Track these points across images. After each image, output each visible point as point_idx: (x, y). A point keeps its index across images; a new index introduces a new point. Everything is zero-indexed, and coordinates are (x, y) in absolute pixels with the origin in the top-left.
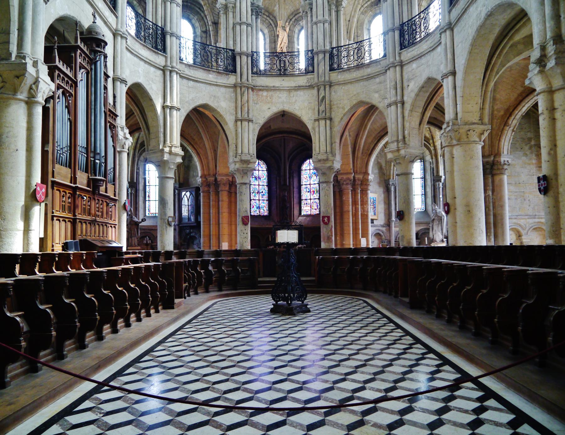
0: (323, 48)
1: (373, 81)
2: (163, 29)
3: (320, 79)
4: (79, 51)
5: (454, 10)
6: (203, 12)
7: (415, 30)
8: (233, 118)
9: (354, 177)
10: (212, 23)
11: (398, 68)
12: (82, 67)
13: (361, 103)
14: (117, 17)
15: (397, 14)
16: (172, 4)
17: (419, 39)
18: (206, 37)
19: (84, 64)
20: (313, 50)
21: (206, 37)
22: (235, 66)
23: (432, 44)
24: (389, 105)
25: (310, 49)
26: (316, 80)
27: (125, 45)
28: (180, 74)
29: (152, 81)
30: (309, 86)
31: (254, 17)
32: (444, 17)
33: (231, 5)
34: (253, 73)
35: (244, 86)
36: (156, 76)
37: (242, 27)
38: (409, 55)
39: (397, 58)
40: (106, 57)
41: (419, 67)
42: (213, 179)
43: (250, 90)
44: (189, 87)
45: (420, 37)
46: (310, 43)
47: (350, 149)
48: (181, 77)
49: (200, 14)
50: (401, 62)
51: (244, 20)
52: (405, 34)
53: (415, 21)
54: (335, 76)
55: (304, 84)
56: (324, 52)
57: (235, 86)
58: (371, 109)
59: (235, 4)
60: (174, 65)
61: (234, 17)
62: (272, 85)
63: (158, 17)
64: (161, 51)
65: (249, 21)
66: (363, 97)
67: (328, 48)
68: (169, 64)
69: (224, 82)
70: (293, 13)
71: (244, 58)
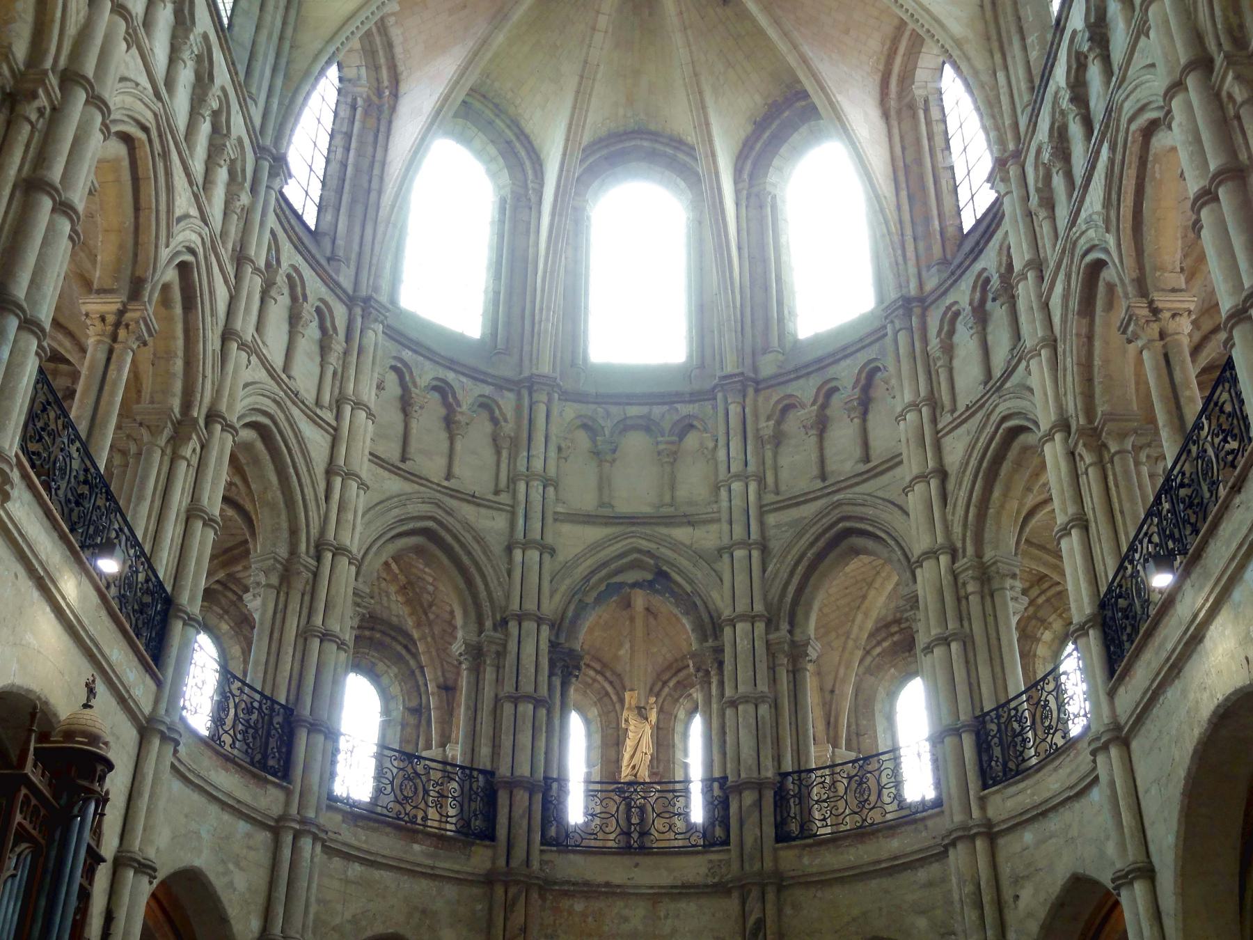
0: (755, 775)
1: (908, 876)
2: (289, 711)
3: (747, 866)
4: (24, 791)
5: (1121, 690)
6: (415, 656)
7: (1020, 734)
10: (439, 687)
11: (979, 843)
12: (22, 835)
14: (159, 684)
16: (326, 644)
17: (1034, 761)
18: (418, 726)
19: (29, 827)
20: (725, 778)
21: (418, 726)
23: (1074, 779)
25: (717, 775)
26: (735, 866)
27: (169, 758)
28: (323, 841)
29: (237, 865)
30: (715, 885)
31: (557, 682)
32: (1096, 706)
33: (494, 648)
34: (545, 841)
35: (517, 882)
36: (250, 848)
37: (521, 708)
38: (1010, 804)
39: (976, 813)
40: (103, 800)
41: (1044, 841)
43: (535, 895)
44: (347, 881)
45: (1037, 754)
46: (716, 757)
48: (327, 849)
49: (407, 663)
50: (989, 824)
51: (527, 687)
52: (995, 744)
53: (1016, 709)
54: (792, 859)
55: (700, 880)
56: (759, 786)
57: (489, 880)
59: (505, 646)
60: (311, 814)
61: (498, 681)
62: (600, 879)
63: (279, 678)
64: (274, 775)
65: (544, 691)
67: (769, 773)
68: (294, 811)
69: (457, 867)
70: (669, 667)
71: (521, 797)
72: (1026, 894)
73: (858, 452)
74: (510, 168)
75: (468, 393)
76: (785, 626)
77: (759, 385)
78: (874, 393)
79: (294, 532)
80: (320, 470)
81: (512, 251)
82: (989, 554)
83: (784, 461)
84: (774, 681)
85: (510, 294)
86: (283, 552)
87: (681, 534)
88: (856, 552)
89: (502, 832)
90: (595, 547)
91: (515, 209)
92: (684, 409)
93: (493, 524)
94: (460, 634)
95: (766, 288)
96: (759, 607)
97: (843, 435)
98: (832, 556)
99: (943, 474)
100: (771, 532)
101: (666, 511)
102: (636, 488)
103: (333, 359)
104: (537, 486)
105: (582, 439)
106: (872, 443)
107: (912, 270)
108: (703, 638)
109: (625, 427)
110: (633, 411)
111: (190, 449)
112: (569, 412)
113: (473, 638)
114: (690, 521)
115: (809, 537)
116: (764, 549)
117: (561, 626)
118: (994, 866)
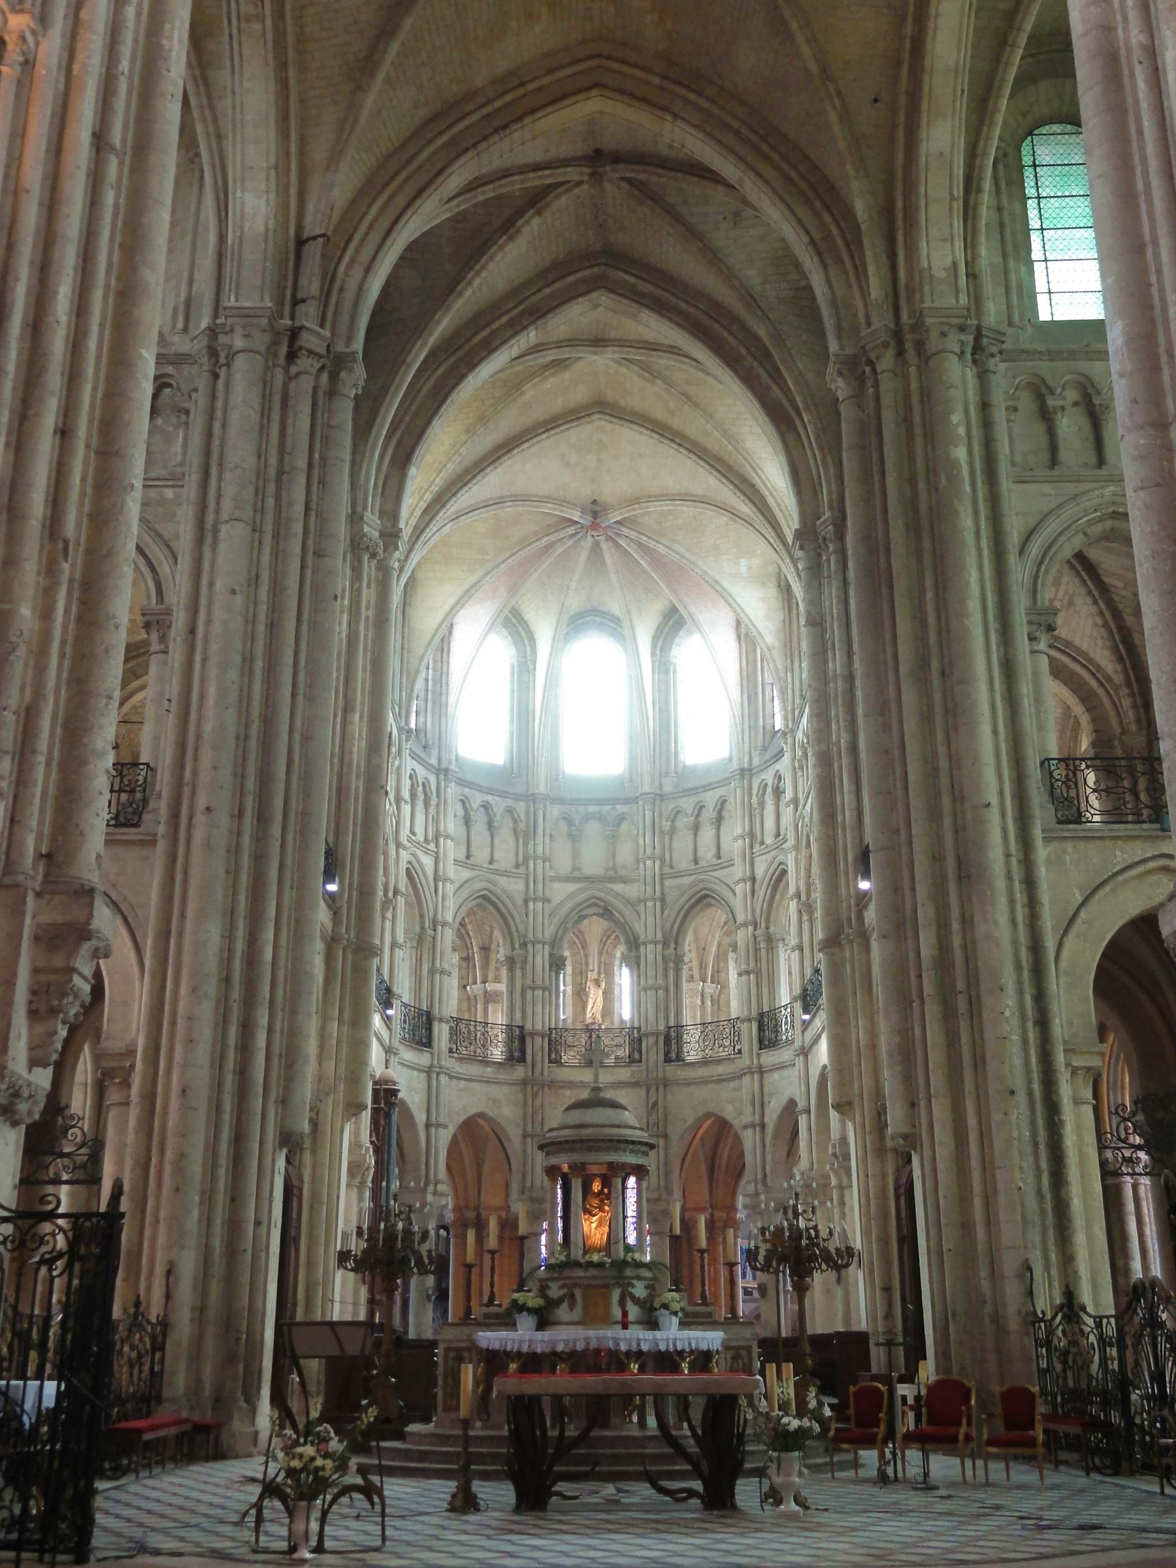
2: (428, 1014)
8: (520, 1131)
9: (712, 1215)
13: (708, 1115)
15: (754, 998)
22: (523, 1051)
24: (746, 1127)
42: (474, 1214)
47: (703, 1169)
48: (451, 1077)
50: (760, 1067)
51: (539, 982)
54: (672, 1071)
56: (657, 1035)
57: (524, 1083)
58: (722, 1129)
61: (524, 976)
66: (711, 1107)
67: (662, 1027)
71: (538, 1040)
72: (773, 1101)
73: (714, 851)
74: (515, 643)
75: (499, 805)
76: (673, 946)
77: (662, 797)
78: (725, 814)
79: (422, 916)
80: (431, 878)
81: (519, 702)
82: (772, 929)
83: (675, 845)
84: (666, 976)
85: (519, 735)
86: (418, 929)
87: (618, 888)
88: (710, 905)
89: (529, 1058)
90: (572, 896)
91: (520, 673)
92: (621, 808)
93: (515, 887)
94: (501, 950)
95: (668, 732)
96: (659, 936)
97: (707, 834)
98: (698, 907)
99: (753, 879)
100: (667, 890)
101: (611, 873)
102: (593, 858)
103: (432, 811)
104: (540, 862)
105: (563, 826)
106: (724, 846)
107: (747, 749)
108: (630, 950)
109: (586, 818)
110: (593, 809)
111: (389, 915)
112: (555, 811)
113: (509, 953)
114: (624, 881)
115: (685, 897)
116: (663, 901)
117: (555, 943)
118: (762, 1086)
